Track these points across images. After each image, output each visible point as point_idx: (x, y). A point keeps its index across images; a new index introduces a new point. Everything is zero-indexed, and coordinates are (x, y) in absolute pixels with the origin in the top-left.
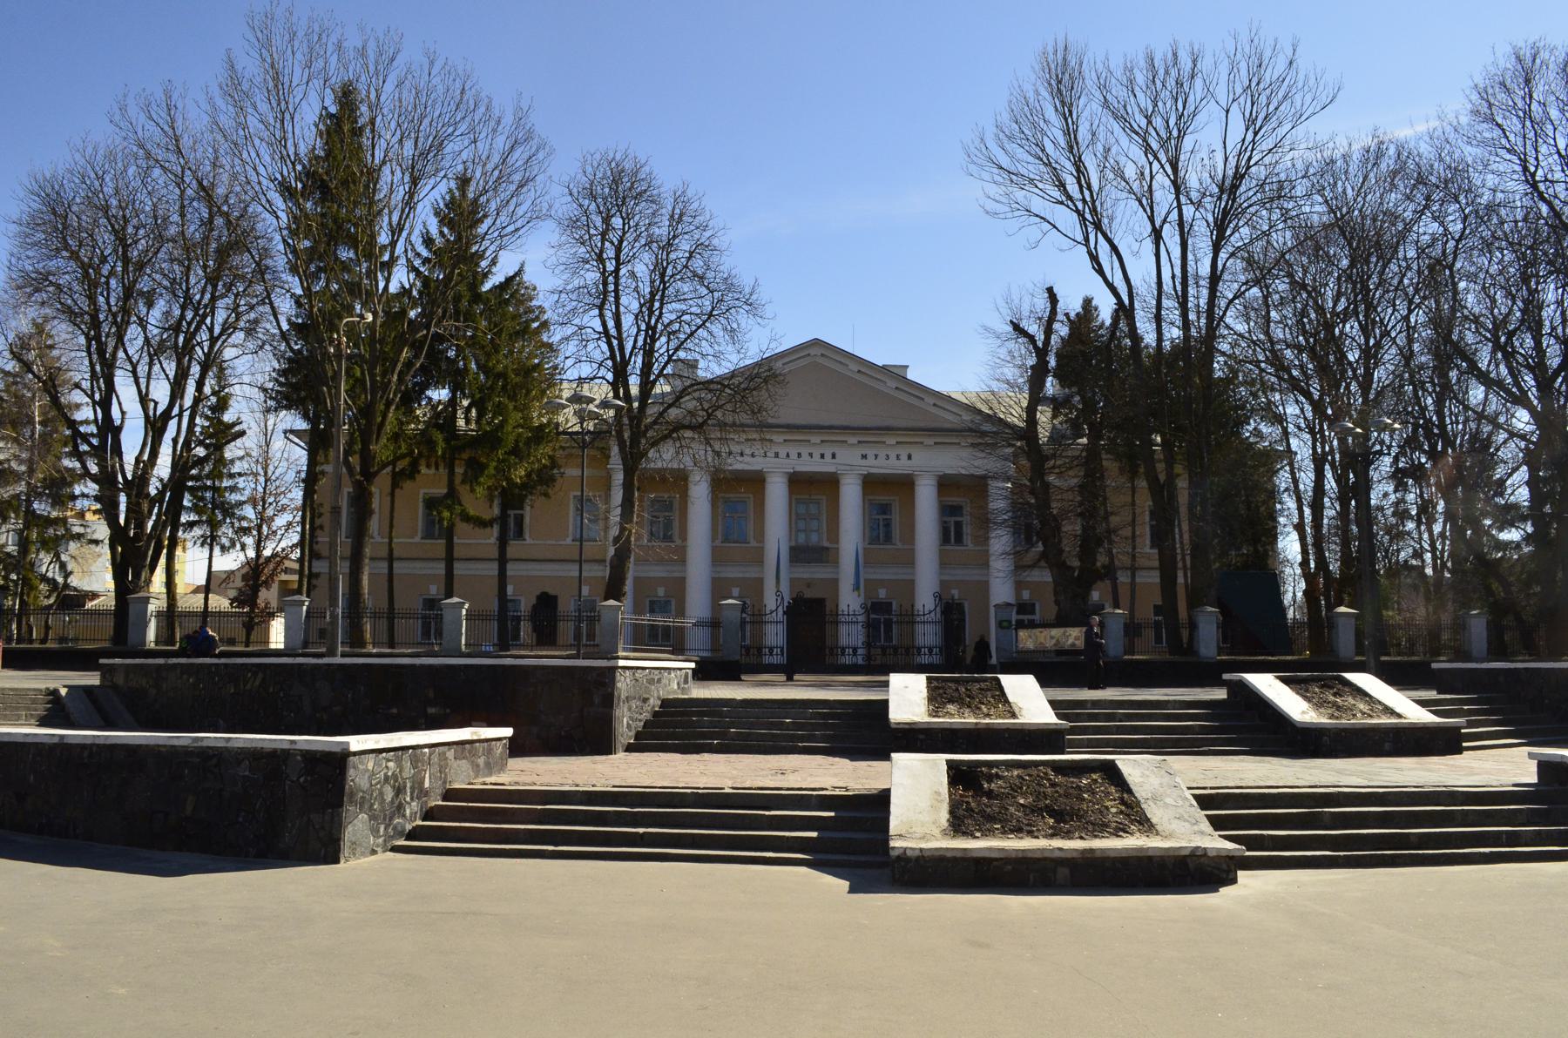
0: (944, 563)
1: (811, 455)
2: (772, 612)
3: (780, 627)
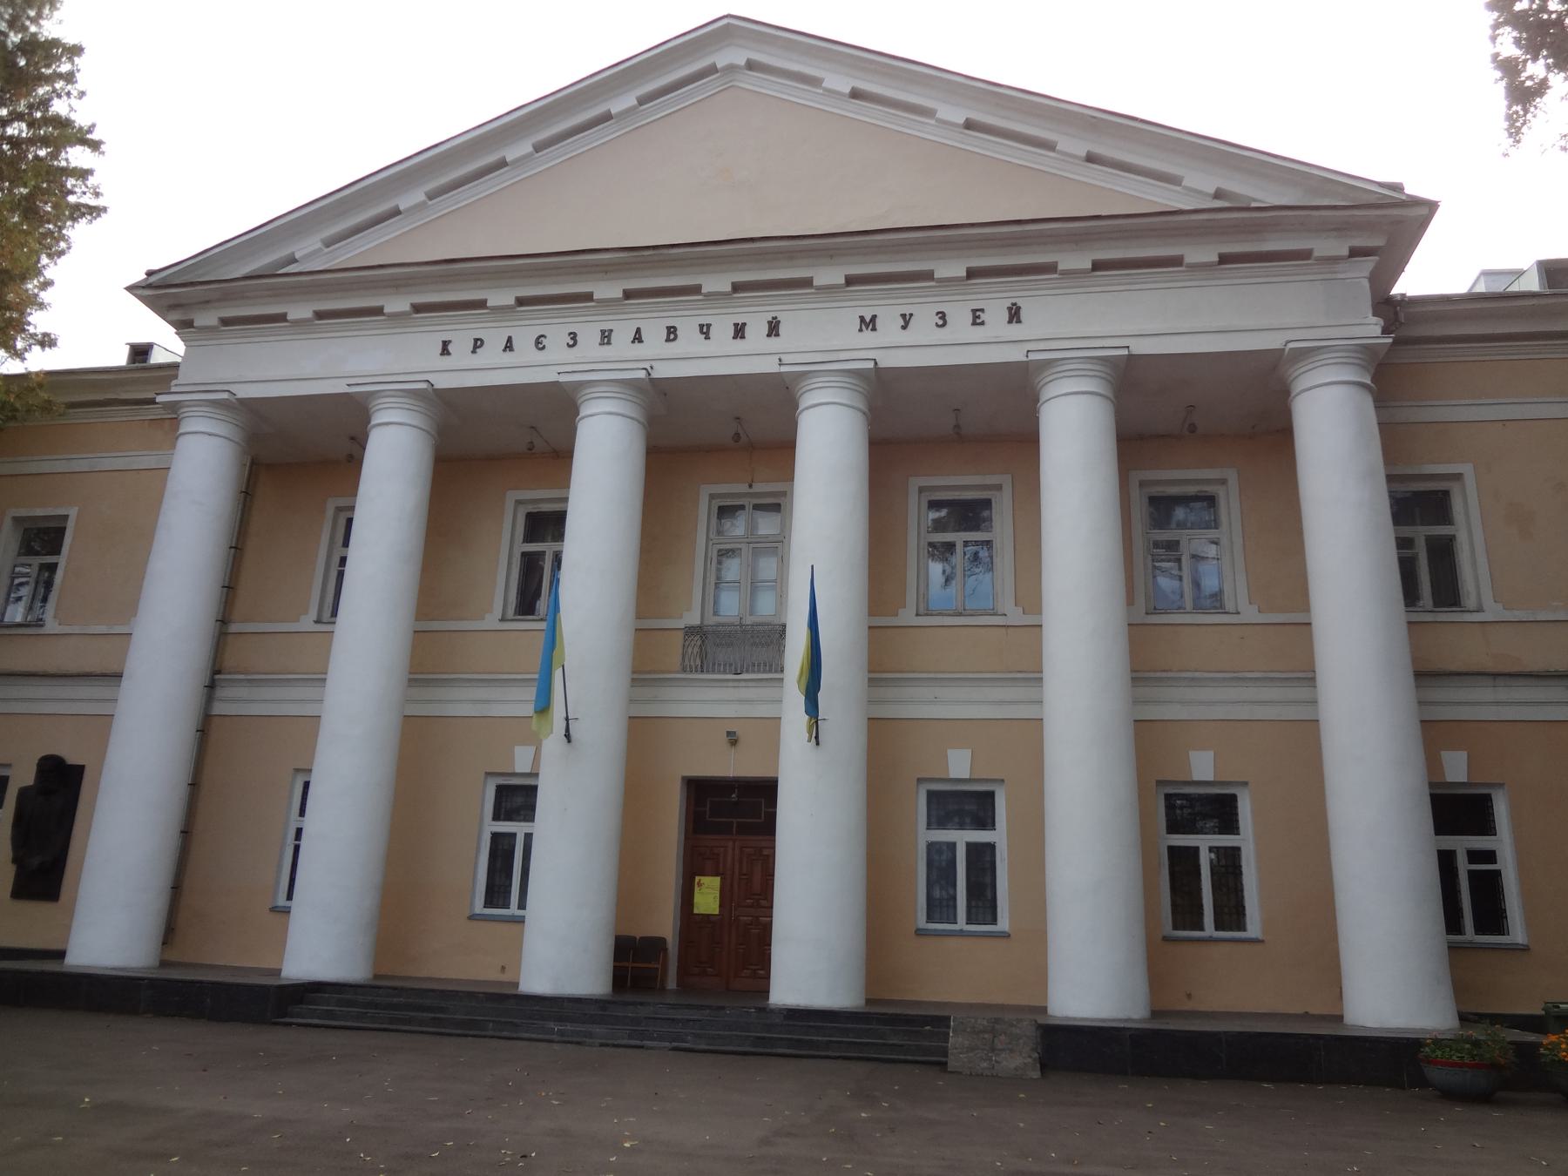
1: (705, 330)
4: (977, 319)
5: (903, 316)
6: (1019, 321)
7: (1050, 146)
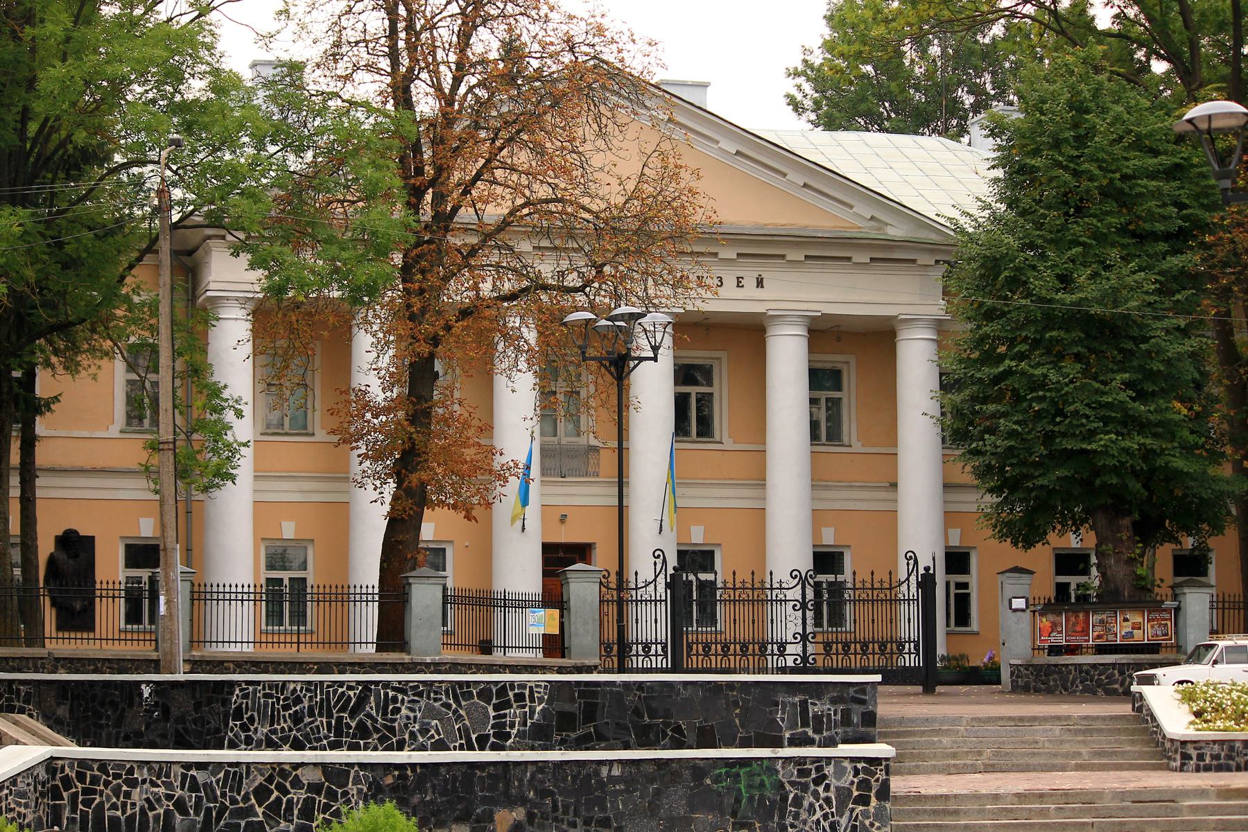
0: (819, 481)
2: (647, 584)
3: (661, 608)
6: (762, 287)
7: (784, 175)
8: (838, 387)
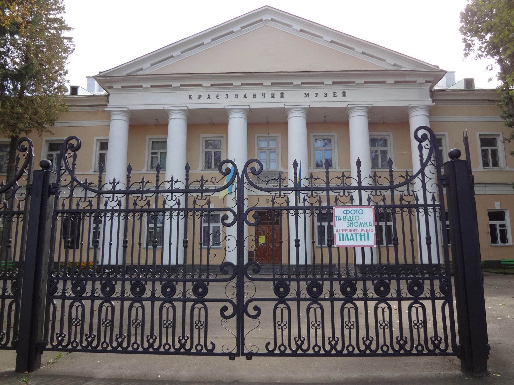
1: (264, 95)
4: (335, 95)
5: (316, 93)
7: (353, 49)
8: (385, 145)
